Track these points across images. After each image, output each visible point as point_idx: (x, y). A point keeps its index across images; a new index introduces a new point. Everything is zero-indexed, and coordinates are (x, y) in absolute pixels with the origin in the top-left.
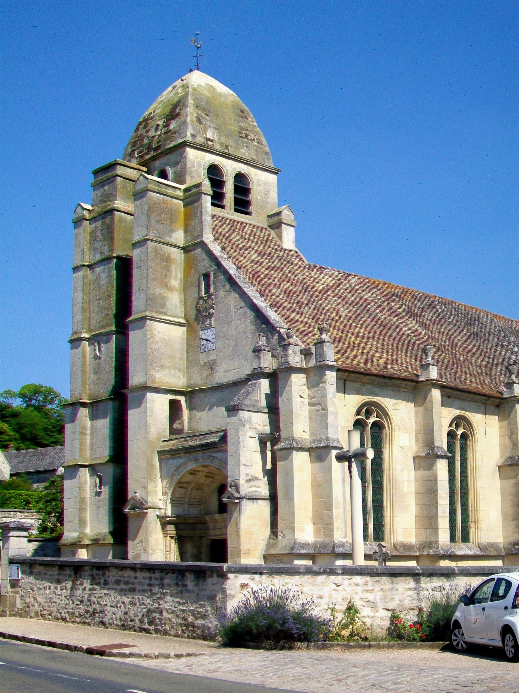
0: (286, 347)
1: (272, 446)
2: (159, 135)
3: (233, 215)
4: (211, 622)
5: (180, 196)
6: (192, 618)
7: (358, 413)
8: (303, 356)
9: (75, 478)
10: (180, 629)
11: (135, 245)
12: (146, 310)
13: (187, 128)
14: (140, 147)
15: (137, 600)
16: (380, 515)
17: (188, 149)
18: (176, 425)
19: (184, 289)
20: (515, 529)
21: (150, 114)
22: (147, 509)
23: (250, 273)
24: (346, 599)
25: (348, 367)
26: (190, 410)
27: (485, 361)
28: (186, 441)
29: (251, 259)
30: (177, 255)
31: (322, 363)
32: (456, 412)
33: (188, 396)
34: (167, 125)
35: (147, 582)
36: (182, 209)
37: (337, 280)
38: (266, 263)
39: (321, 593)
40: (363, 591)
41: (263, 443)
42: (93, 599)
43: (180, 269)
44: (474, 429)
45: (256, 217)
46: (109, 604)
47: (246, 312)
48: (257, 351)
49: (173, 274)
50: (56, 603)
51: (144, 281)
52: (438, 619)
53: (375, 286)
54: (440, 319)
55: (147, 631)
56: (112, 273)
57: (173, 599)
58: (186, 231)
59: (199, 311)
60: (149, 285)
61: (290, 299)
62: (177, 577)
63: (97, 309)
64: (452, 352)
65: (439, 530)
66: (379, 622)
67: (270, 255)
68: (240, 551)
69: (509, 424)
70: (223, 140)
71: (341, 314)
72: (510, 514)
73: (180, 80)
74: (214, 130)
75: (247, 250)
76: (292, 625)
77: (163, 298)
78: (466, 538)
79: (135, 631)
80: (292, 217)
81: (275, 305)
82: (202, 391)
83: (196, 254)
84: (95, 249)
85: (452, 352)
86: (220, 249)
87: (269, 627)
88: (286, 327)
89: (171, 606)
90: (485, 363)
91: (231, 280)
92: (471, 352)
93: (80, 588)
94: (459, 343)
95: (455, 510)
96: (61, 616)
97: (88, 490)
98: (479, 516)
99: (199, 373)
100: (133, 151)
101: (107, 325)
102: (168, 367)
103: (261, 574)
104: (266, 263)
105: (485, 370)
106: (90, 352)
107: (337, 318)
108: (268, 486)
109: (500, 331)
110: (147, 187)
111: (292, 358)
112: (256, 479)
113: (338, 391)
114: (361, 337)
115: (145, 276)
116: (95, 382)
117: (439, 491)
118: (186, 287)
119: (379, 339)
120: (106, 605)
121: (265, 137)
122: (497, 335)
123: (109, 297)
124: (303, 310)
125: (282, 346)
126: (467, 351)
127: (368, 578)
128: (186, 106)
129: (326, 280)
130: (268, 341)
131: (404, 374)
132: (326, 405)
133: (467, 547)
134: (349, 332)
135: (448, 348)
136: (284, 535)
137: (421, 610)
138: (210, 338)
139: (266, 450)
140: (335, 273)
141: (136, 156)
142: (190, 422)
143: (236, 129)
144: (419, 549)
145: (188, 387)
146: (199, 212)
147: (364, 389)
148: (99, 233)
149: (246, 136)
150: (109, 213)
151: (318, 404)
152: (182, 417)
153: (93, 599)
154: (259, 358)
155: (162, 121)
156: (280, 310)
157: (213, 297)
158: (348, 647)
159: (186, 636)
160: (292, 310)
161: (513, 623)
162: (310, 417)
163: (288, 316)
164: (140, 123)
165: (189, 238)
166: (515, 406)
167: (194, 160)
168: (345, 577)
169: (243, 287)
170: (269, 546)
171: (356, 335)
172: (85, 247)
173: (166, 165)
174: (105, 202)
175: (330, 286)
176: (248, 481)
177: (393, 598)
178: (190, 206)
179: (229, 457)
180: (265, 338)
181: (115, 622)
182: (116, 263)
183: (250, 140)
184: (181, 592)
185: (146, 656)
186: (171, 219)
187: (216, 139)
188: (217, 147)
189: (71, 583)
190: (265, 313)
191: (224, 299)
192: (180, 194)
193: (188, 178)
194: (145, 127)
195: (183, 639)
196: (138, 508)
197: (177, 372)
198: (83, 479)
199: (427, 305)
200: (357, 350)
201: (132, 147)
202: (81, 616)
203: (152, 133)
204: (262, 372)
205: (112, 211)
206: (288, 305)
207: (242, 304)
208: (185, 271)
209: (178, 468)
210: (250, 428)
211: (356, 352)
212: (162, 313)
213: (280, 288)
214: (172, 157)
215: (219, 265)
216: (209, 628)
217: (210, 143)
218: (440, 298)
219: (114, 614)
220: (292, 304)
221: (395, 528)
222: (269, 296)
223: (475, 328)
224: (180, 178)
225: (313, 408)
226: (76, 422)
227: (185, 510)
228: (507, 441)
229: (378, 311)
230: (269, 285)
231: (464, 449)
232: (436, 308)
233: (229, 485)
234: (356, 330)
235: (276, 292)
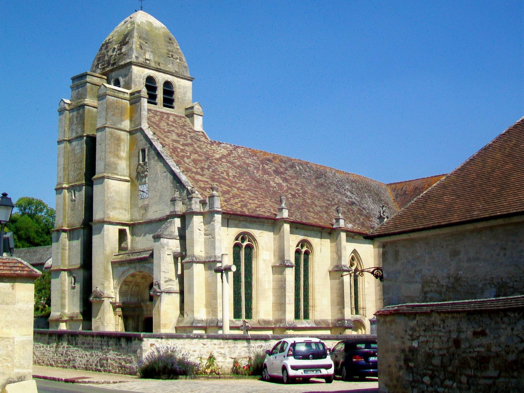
0: (190, 199)
1: (182, 260)
2: (115, 55)
3: (162, 109)
4: (134, 365)
5: (128, 98)
6: (124, 363)
7: (237, 239)
8: (201, 204)
9: (58, 278)
10: (118, 369)
11: (98, 130)
12: (104, 172)
13: (133, 52)
14: (103, 61)
15: (94, 353)
16: (250, 303)
17: (133, 67)
18: (123, 245)
19: (129, 158)
20: (338, 311)
21: (110, 39)
22: (104, 298)
23: (171, 149)
24: (209, 352)
25: (230, 211)
26: (132, 236)
27: (325, 203)
28: (129, 256)
29: (172, 139)
30: (125, 136)
31: (213, 209)
32: (301, 238)
33: (131, 227)
34: (120, 49)
35: (100, 343)
36: (129, 106)
37: (229, 151)
38: (182, 141)
39: (195, 349)
40: (218, 348)
41: (176, 258)
42: (69, 353)
43: (127, 145)
44: (313, 248)
45: (177, 109)
46: (78, 356)
47: (167, 175)
48: (173, 200)
49: (122, 148)
50: (47, 355)
51: (104, 154)
52: (258, 363)
53: (254, 154)
54: (298, 175)
55: (99, 371)
56: (83, 145)
57: (114, 352)
58: (131, 121)
59: (138, 173)
60: (106, 156)
61: (196, 166)
62: (116, 341)
63: (73, 169)
64: (303, 197)
66: (227, 365)
67: (185, 135)
68: (160, 325)
69: (337, 245)
70: (156, 59)
71: (230, 174)
72: (336, 301)
73: (129, 17)
74: (150, 53)
75: (170, 133)
76: (177, 366)
77: (116, 164)
78: (306, 317)
79: (93, 371)
80: (201, 110)
81: (187, 171)
82: (140, 224)
83: (137, 136)
84: (72, 130)
85: (303, 197)
86: (152, 133)
87: (165, 368)
88: (192, 186)
89: (113, 356)
90: (325, 204)
91: (159, 155)
92: (317, 197)
93: (61, 347)
94: (309, 191)
95: (300, 299)
96: (50, 363)
97: (67, 285)
98: (315, 303)
99: (138, 212)
100: (98, 64)
101: (80, 180)
102: (118, 208)
103: (162, 338)
104: (182, 141)
105: (324, 208)
106: (68, 196)
107: (227, 177)
108: (178, 285)
109: (339, 181)
110: (105, 93)
111: (194, 205)
112: (171, 280)
113: (223, 225)
114: (241, 190)
115: (104, 150)
116: (71, 216)
118: (130, 157)
119: (253, 190)
120: (76, 356)
121: (185, 56)
122: (337, 184)
123: (81, 162)
124: (204, 173)
125: (188, 198)
126: (313, 196)
127: (221, 341)
128: (133, 37)
129: (221, 151)
130: (180, 194)
131: (267, 214)
132: (215, 236)
133: (307, 322)
134: (234, 187)
135: (301, 195)
136: (188, 315)
137: (250, 358)
138: (145, 190)
139: (178, 262)
140: (228, 146)
141: (100, 67)
142: (132, 243)
143: (166, 52)
144: (274, 324)
145: (131, 220)
146: (139, 109)
147: (240, 225)
148: (75, 120)
149: (172, 56)
150: (82, 107)
151: (210, 234)
152: (127, 240)
153: (69, 353)
154: (174, 205)
155: (117, 45)
156: (189, 174)
157: (147, 164)
158: (208, 378)
159: (121, 373)
160: (197, 173)
161: (287, 364)
162: (205, 242)
163: (194, 177)
164: (103, 45)
165: (133, 125)
166: (340, 233)
167: (137, 73)
168: (208, 340)
169: (166, 159)
170: (179, 321)
171: (238, 189)
172: (66, 128)
173: (119, 76)
174: (79, 99)
175: (224, 155)
176: (166, 282)
177: (235, 352)
178: (134, 105)
179: (154, 266)
180: (178, 192)
181: (81, 366)
182: (85, 140)
183: (174, 58)
184: (119, 349)
185: (97, 383)
186: (121, 112)
187: (152, 59)
188: (153, 64)
189: (56, 344)
190: (179, 176)
191: (154, 166)
192: (128, 96)
193: (133, 86)
194: (106, 48)
195: (119, 375)
196: (98, 297)
197: (124, 211)
198: (64, 278)
199: (289, 166)
200: (238, 199)
201: (97, 61)
202: (61, 363)
203: (110, 53)
204: (176, 214)
205: (83, 106)
206: (194, 170)
207: (165, 170)
208: (130, 147)
209: (123, 273)
210: (168, 249)
211: (237, 201)
212: (114, 174)
213: (190, 158)
214: (122, 71)
215: (151, 144)
216: (133, 368)
217: (148, 62)
218: (299, 160)
219: (81, 361)
220: (197, 169)
222: (182, 164)
223: (321, 181)
224: (128, 86)
225: (207, 237)
226: (59, 242)
227: (128, 299)
228: (335, 256)
229: (255, 171)
230: (183, 157)
231: (306, 261)
232: (296, 167)
233: (154, 284)
234: (239, 185)
235: (187, 161)
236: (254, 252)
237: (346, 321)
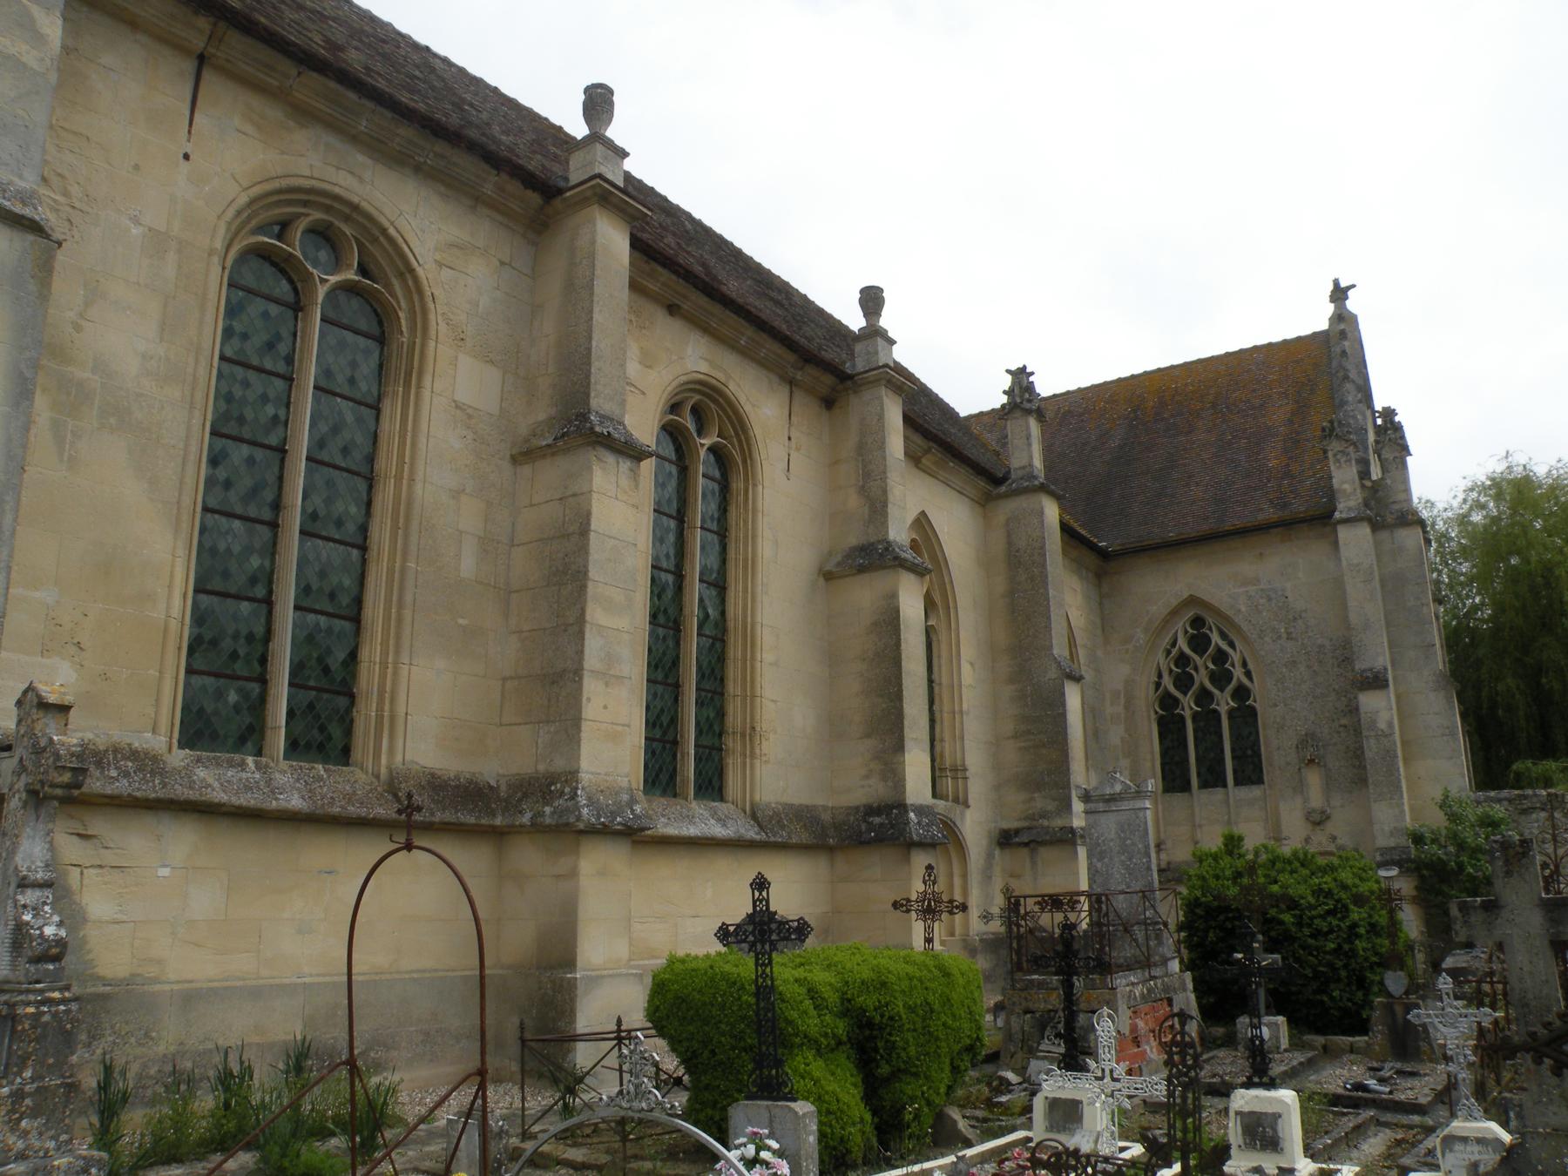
65: (585, 726)
78: (711, 785)
117: (593, 573)
221: (401, 710)
228: (853, 501)
236: (394, 346)
237: (912, 815)
